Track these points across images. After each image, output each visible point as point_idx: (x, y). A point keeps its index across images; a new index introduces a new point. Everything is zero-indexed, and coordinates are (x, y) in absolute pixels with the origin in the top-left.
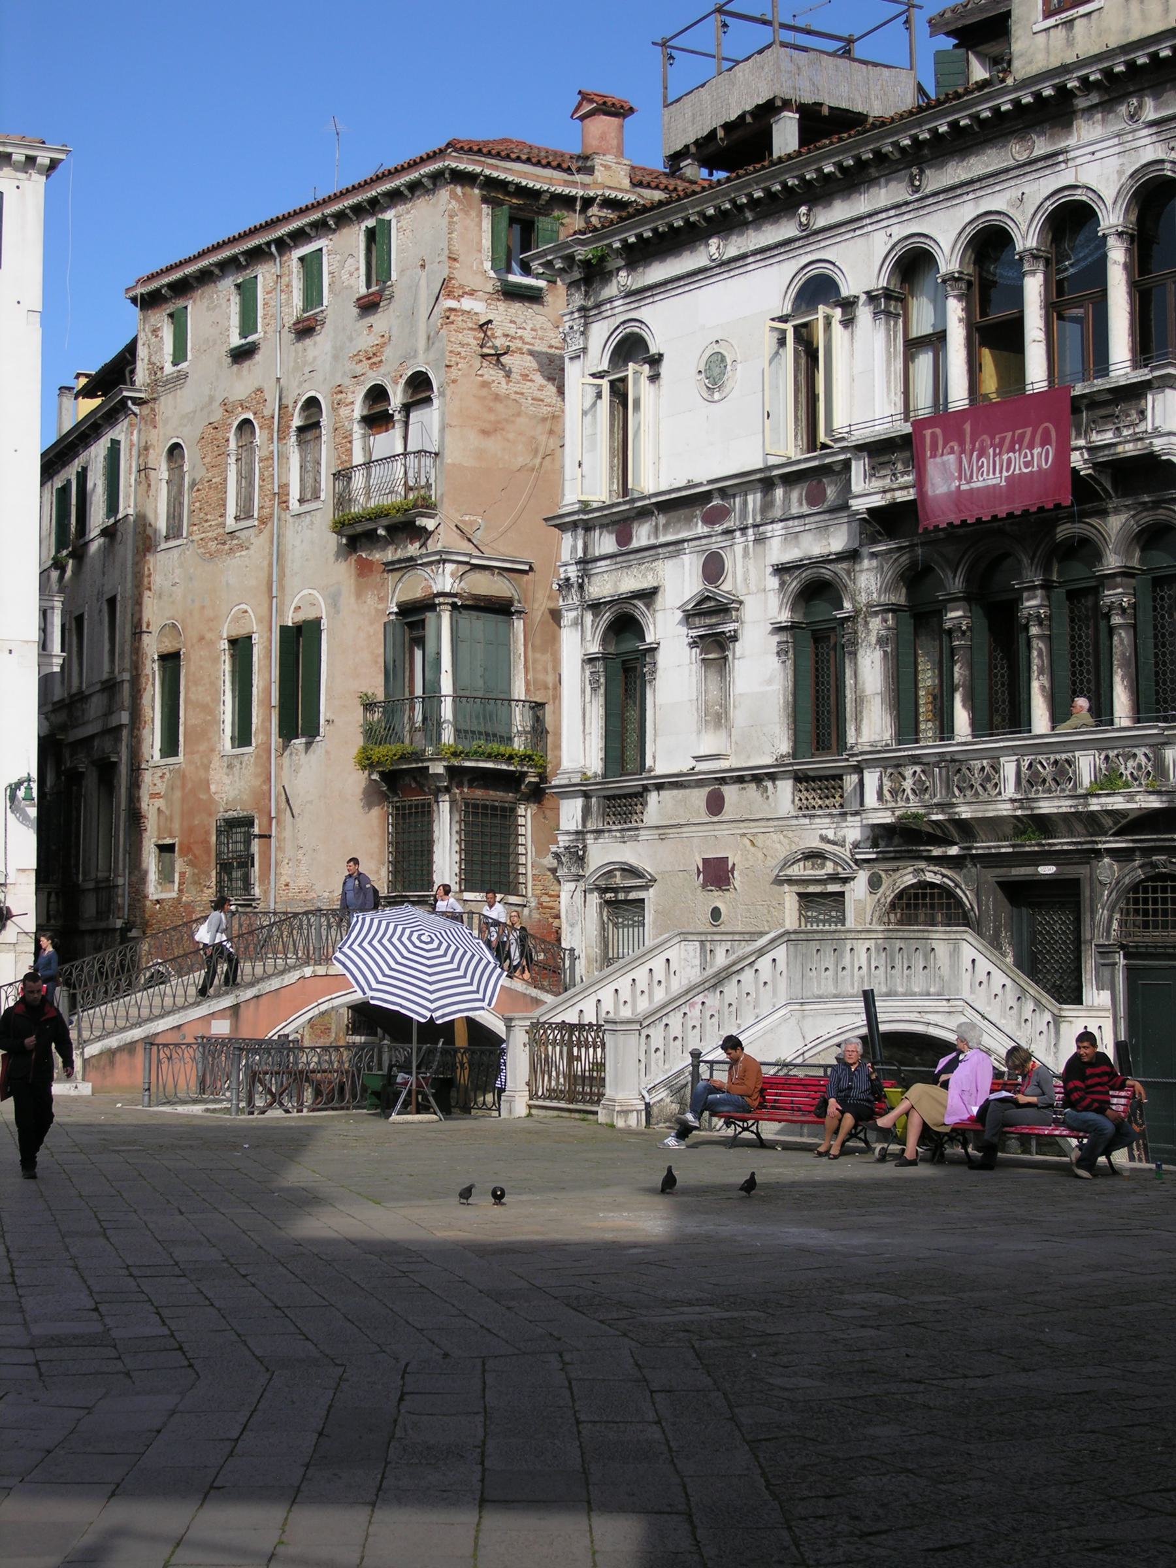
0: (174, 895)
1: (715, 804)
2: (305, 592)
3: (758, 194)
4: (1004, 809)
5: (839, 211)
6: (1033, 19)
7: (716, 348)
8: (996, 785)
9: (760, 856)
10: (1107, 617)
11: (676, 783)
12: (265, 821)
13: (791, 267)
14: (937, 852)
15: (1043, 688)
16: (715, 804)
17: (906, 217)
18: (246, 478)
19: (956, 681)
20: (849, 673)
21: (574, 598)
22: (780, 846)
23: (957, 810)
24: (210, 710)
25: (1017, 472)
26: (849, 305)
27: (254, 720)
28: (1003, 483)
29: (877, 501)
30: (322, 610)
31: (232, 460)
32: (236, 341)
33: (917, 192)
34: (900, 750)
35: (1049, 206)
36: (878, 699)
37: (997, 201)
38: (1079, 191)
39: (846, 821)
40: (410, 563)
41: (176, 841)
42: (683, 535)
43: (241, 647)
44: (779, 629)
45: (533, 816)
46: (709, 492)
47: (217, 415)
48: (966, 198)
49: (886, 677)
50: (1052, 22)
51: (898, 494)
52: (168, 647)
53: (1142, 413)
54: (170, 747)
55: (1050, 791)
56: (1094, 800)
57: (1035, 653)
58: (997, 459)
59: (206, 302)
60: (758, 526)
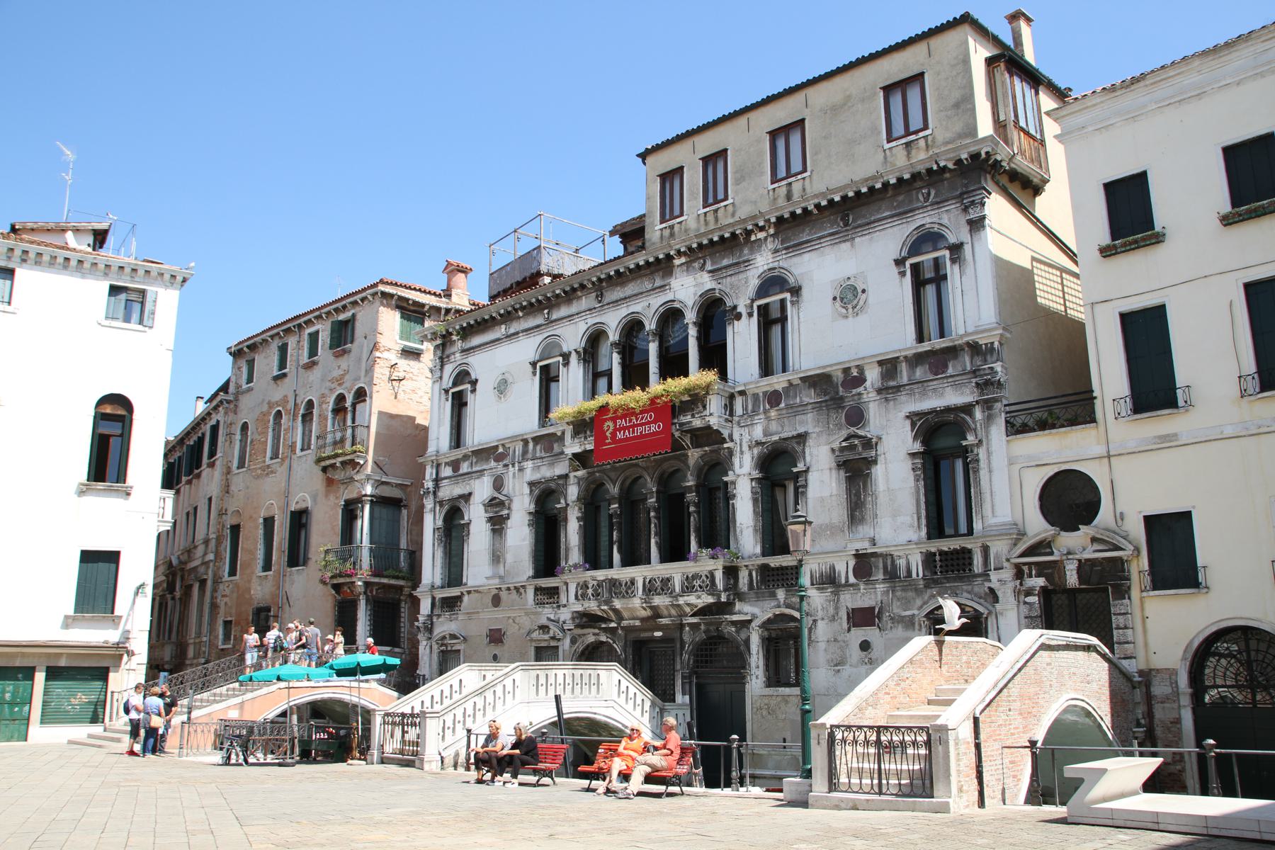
0: (230, 646)
1: (496, 601)
2: (301, 494)
3: (524, 303)
12: (276, 608)
13: (539, 338)
14: (603, 626)
15: (656, 543)
16: (496, 601)
18: (277, 438)
19: (614, 539)
20: (562, 535)
22: (527, 623)
24: (252, 553)
26: (566, 357)
27: (274, 558)
29: (577, 449)
30: (309, 504)
31: (270, 430)
32: (276, 373)
35: (662, 310)
36: (577, 548)
37: (637, 307)
41: (233, 619)
42: (485, 467)
43: (269, 522)
45: (409, 608)
46: (497, 446)
47: (265, 408)
49: (580, 539)
50: (664, 225)
52: (234, 521)
53: (704, 407)
54: (233, 572)
55: (660, 594)
56: (680, 599)
57: (653, 525)
59: (264, 354)
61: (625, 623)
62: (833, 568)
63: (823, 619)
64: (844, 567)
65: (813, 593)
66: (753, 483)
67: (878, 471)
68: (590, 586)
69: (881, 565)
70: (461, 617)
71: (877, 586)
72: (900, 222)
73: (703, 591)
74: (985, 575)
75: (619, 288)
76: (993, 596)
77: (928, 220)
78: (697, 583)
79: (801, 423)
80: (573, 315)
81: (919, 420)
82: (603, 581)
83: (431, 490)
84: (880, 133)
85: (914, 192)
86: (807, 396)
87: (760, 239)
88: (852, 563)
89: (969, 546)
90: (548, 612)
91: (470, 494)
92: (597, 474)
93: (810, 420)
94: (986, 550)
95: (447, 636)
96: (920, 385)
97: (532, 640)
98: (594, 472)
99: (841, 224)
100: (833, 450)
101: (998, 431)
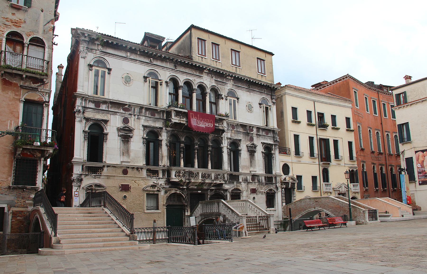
4: (200, 181)
5: (159, 63)
6: (196, 53)
7: (128, 75)
9: (137, 185)
10: (208, 152)
11: (114, 166)
14: (181, 187)
16: (125, 172)
17: (173, 72)
21: (81, 115)
25: (207, 126)
28: (205, 127)
29: (177, 121)
33: (176, 69)
34: (198, 169)
36: (166, 158)
38: (204, 84)
39: (159, 180)
40: (35, 90)
44: (143, 138)
46: (127, 104)
48: (185, 75)
51: (181, 121)
53: (223, 123)
56: (215, 181)
58: (204, 123)
60: (139, 116)
63: (245, 191)
64: (249, 178)
66: (228, 150)
67: (256, 154)
68: (181, 172)
69: (257, 178)
70: (102, 177)
71: (256, 183)
72: (260, 94)
73: (221, 179)
74: (276, 183)
75: (183, 68)
76: (277, 188)
77: (264, 97)
78: (219, 177)
79: (240, 136)
80: (165, 67)
81: (264, 145)
82: (187, 172)
83: (82, 111)
84: (256, 69)
85: (262, 88)
88: (251, 177)
89: (273, 177)
90: (153, 181)
91: (108, 121)
92: (176, 132)
93: (242, 136)
94: (276, 178)
95: (94, 186)
96: (264, 136)
97: (147, 191)
98: (175, 131)
99: (248, 87)
100: (247, 146)
101: (277, 152)
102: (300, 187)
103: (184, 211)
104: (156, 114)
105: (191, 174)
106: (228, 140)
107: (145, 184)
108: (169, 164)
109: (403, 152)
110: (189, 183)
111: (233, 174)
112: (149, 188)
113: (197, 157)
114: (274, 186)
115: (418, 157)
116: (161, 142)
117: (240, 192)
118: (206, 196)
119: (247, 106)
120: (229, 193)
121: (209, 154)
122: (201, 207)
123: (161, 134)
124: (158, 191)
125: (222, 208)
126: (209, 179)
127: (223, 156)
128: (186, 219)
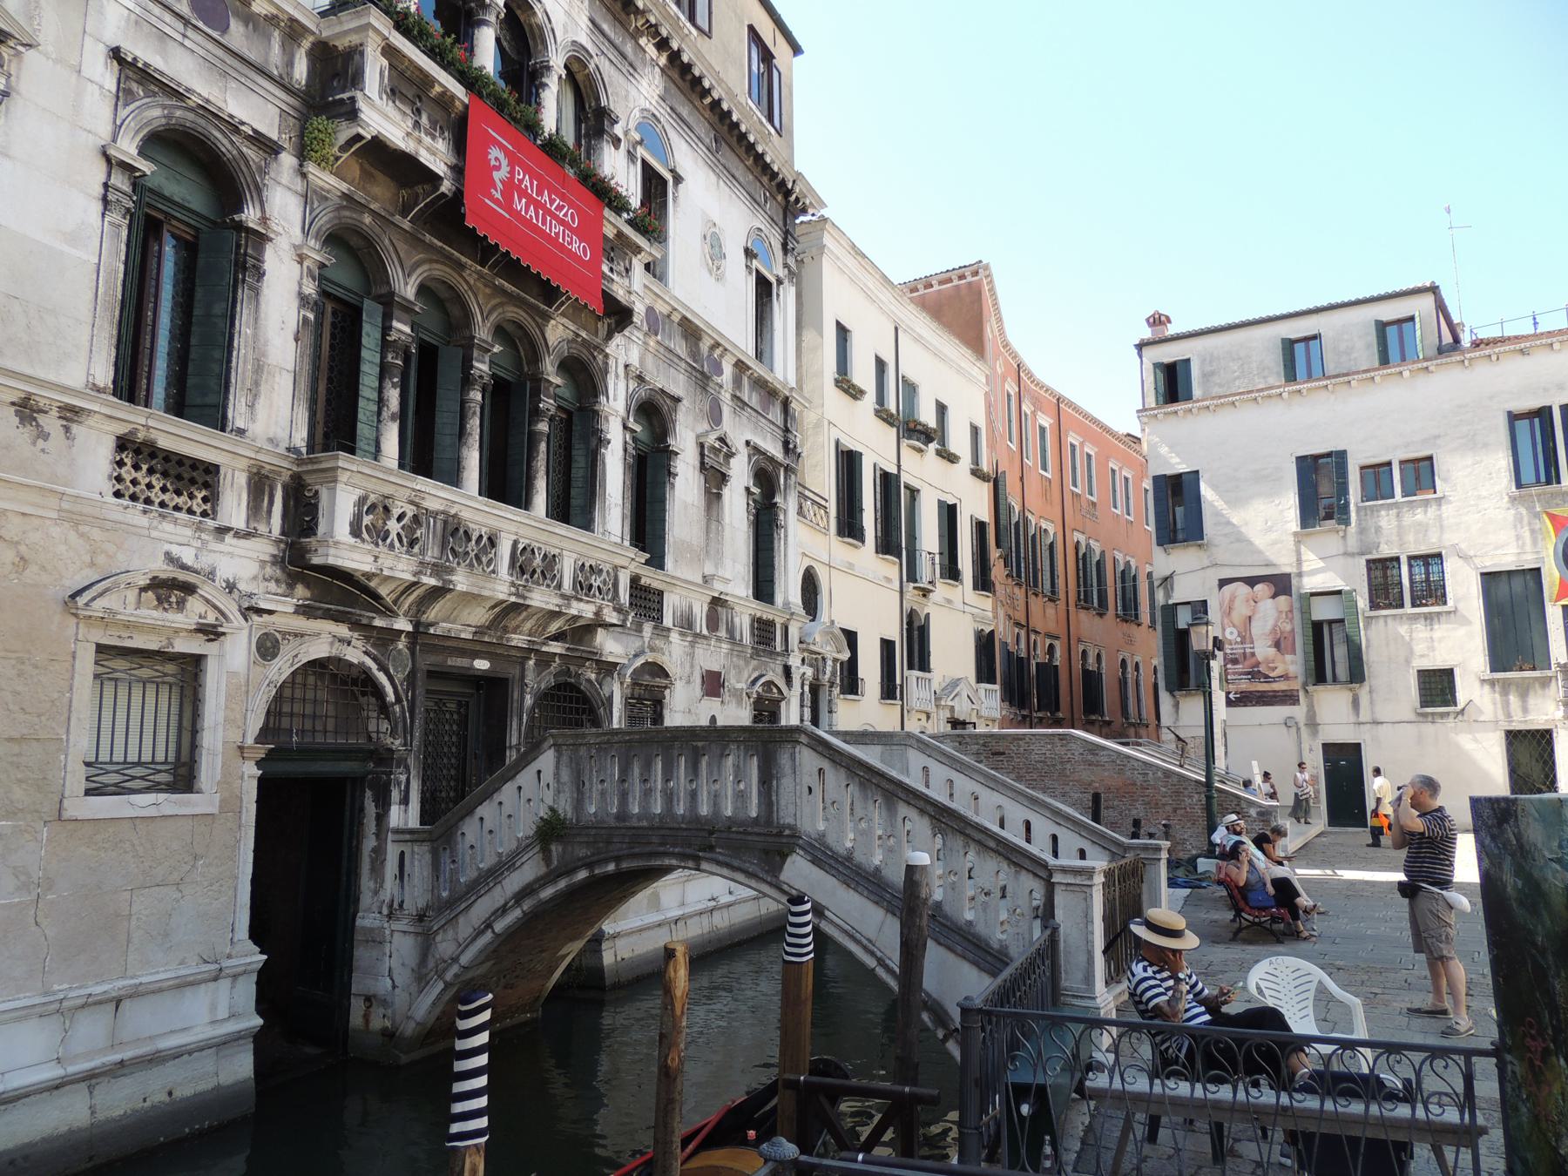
8: (490, 562)
14: (378, 622)
23: (454, 578)
56: (574, 603)
61: (442, 628)
62: (691, 608)
64: (700, 611)
65: (674, 637)
68: (396, 512)
77: (763, 227)
82: (435, 514)
86: (680, 347)
87: (645, 51)
88: (706, 608)
92: (367, 219)
98: (364, 207)
102: (851, 683)
103: (376, 801)
104: (236, 27)
105: (452, 535)
106: (633, 385)
107: (92, 564)
108: (304, 434)
109: (1166, 579)
110: (436, 593)
111: (642, 582)
112: (132, 595)
113: (477, 437)
114: (780, 670)
115: (1232, 600)
116: (260, 249)
117: (666, 687)
118: (516, 695)
119: (705, 237)
120: (622, 683)
121: (541, 433)
122: (557, 775)
123: (265, 193)
124: (211, 632)
125: (817, 791)
126: (548, 586)
127: (604, 463)
128: (392, 852)
